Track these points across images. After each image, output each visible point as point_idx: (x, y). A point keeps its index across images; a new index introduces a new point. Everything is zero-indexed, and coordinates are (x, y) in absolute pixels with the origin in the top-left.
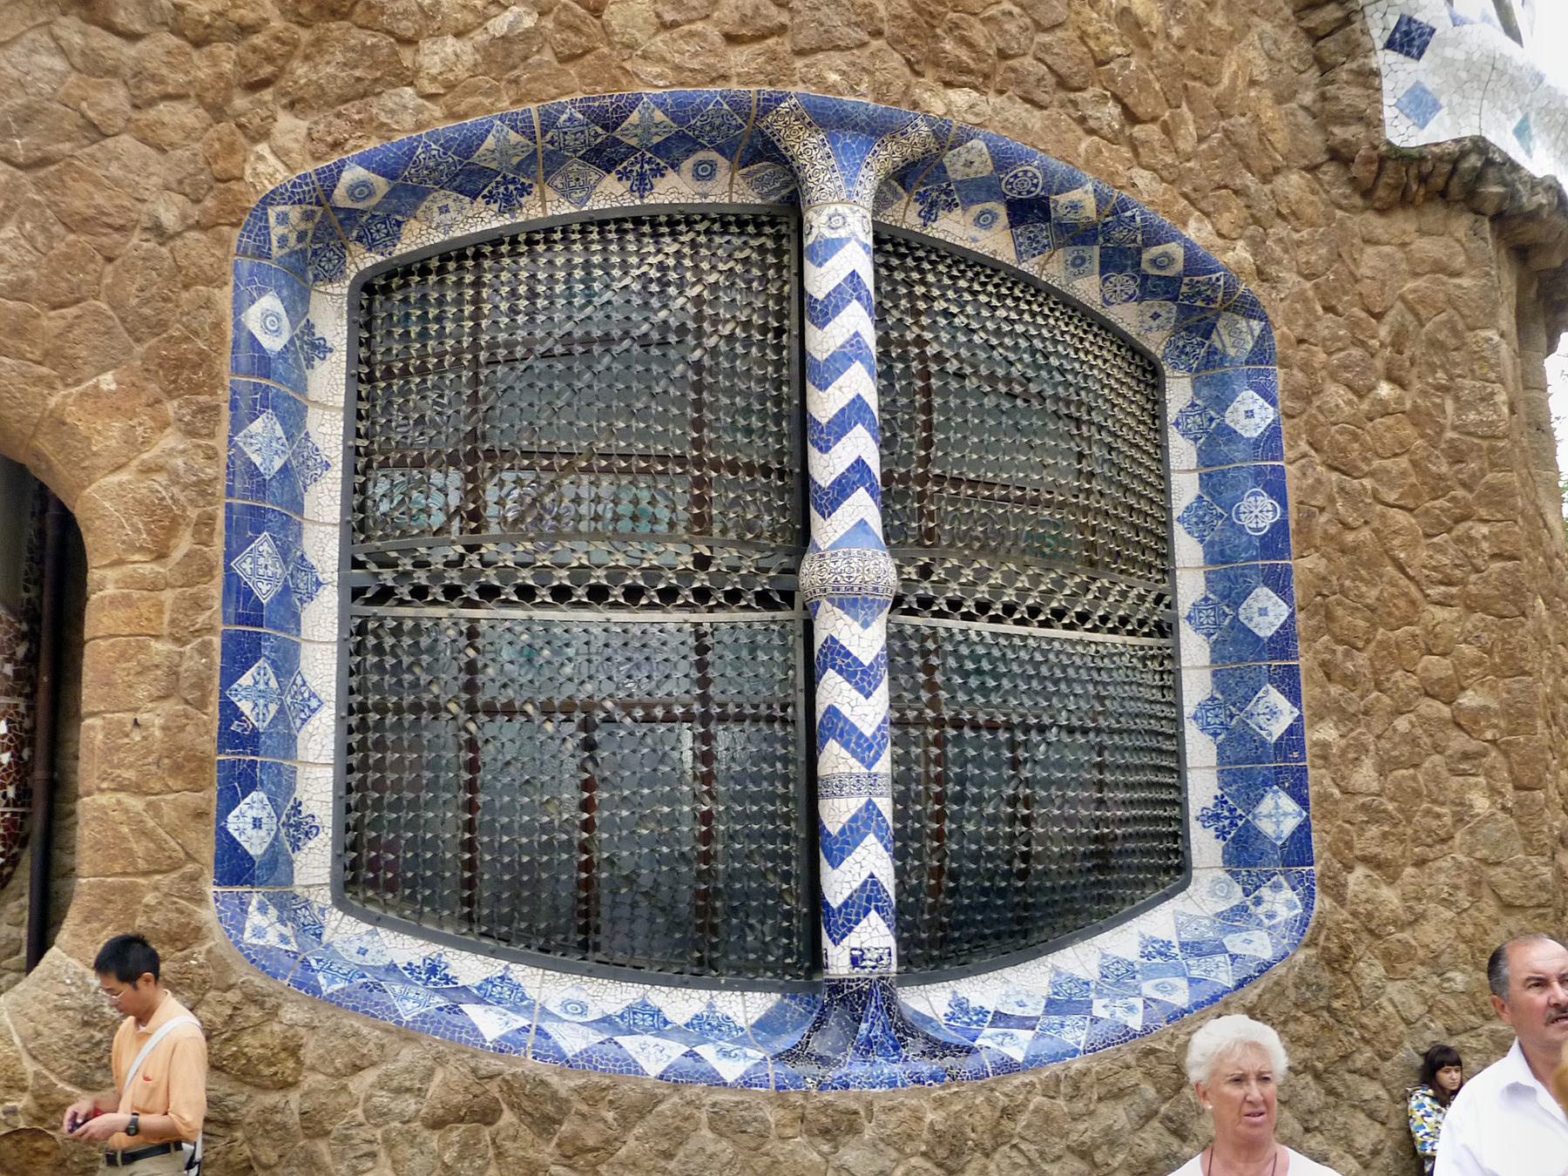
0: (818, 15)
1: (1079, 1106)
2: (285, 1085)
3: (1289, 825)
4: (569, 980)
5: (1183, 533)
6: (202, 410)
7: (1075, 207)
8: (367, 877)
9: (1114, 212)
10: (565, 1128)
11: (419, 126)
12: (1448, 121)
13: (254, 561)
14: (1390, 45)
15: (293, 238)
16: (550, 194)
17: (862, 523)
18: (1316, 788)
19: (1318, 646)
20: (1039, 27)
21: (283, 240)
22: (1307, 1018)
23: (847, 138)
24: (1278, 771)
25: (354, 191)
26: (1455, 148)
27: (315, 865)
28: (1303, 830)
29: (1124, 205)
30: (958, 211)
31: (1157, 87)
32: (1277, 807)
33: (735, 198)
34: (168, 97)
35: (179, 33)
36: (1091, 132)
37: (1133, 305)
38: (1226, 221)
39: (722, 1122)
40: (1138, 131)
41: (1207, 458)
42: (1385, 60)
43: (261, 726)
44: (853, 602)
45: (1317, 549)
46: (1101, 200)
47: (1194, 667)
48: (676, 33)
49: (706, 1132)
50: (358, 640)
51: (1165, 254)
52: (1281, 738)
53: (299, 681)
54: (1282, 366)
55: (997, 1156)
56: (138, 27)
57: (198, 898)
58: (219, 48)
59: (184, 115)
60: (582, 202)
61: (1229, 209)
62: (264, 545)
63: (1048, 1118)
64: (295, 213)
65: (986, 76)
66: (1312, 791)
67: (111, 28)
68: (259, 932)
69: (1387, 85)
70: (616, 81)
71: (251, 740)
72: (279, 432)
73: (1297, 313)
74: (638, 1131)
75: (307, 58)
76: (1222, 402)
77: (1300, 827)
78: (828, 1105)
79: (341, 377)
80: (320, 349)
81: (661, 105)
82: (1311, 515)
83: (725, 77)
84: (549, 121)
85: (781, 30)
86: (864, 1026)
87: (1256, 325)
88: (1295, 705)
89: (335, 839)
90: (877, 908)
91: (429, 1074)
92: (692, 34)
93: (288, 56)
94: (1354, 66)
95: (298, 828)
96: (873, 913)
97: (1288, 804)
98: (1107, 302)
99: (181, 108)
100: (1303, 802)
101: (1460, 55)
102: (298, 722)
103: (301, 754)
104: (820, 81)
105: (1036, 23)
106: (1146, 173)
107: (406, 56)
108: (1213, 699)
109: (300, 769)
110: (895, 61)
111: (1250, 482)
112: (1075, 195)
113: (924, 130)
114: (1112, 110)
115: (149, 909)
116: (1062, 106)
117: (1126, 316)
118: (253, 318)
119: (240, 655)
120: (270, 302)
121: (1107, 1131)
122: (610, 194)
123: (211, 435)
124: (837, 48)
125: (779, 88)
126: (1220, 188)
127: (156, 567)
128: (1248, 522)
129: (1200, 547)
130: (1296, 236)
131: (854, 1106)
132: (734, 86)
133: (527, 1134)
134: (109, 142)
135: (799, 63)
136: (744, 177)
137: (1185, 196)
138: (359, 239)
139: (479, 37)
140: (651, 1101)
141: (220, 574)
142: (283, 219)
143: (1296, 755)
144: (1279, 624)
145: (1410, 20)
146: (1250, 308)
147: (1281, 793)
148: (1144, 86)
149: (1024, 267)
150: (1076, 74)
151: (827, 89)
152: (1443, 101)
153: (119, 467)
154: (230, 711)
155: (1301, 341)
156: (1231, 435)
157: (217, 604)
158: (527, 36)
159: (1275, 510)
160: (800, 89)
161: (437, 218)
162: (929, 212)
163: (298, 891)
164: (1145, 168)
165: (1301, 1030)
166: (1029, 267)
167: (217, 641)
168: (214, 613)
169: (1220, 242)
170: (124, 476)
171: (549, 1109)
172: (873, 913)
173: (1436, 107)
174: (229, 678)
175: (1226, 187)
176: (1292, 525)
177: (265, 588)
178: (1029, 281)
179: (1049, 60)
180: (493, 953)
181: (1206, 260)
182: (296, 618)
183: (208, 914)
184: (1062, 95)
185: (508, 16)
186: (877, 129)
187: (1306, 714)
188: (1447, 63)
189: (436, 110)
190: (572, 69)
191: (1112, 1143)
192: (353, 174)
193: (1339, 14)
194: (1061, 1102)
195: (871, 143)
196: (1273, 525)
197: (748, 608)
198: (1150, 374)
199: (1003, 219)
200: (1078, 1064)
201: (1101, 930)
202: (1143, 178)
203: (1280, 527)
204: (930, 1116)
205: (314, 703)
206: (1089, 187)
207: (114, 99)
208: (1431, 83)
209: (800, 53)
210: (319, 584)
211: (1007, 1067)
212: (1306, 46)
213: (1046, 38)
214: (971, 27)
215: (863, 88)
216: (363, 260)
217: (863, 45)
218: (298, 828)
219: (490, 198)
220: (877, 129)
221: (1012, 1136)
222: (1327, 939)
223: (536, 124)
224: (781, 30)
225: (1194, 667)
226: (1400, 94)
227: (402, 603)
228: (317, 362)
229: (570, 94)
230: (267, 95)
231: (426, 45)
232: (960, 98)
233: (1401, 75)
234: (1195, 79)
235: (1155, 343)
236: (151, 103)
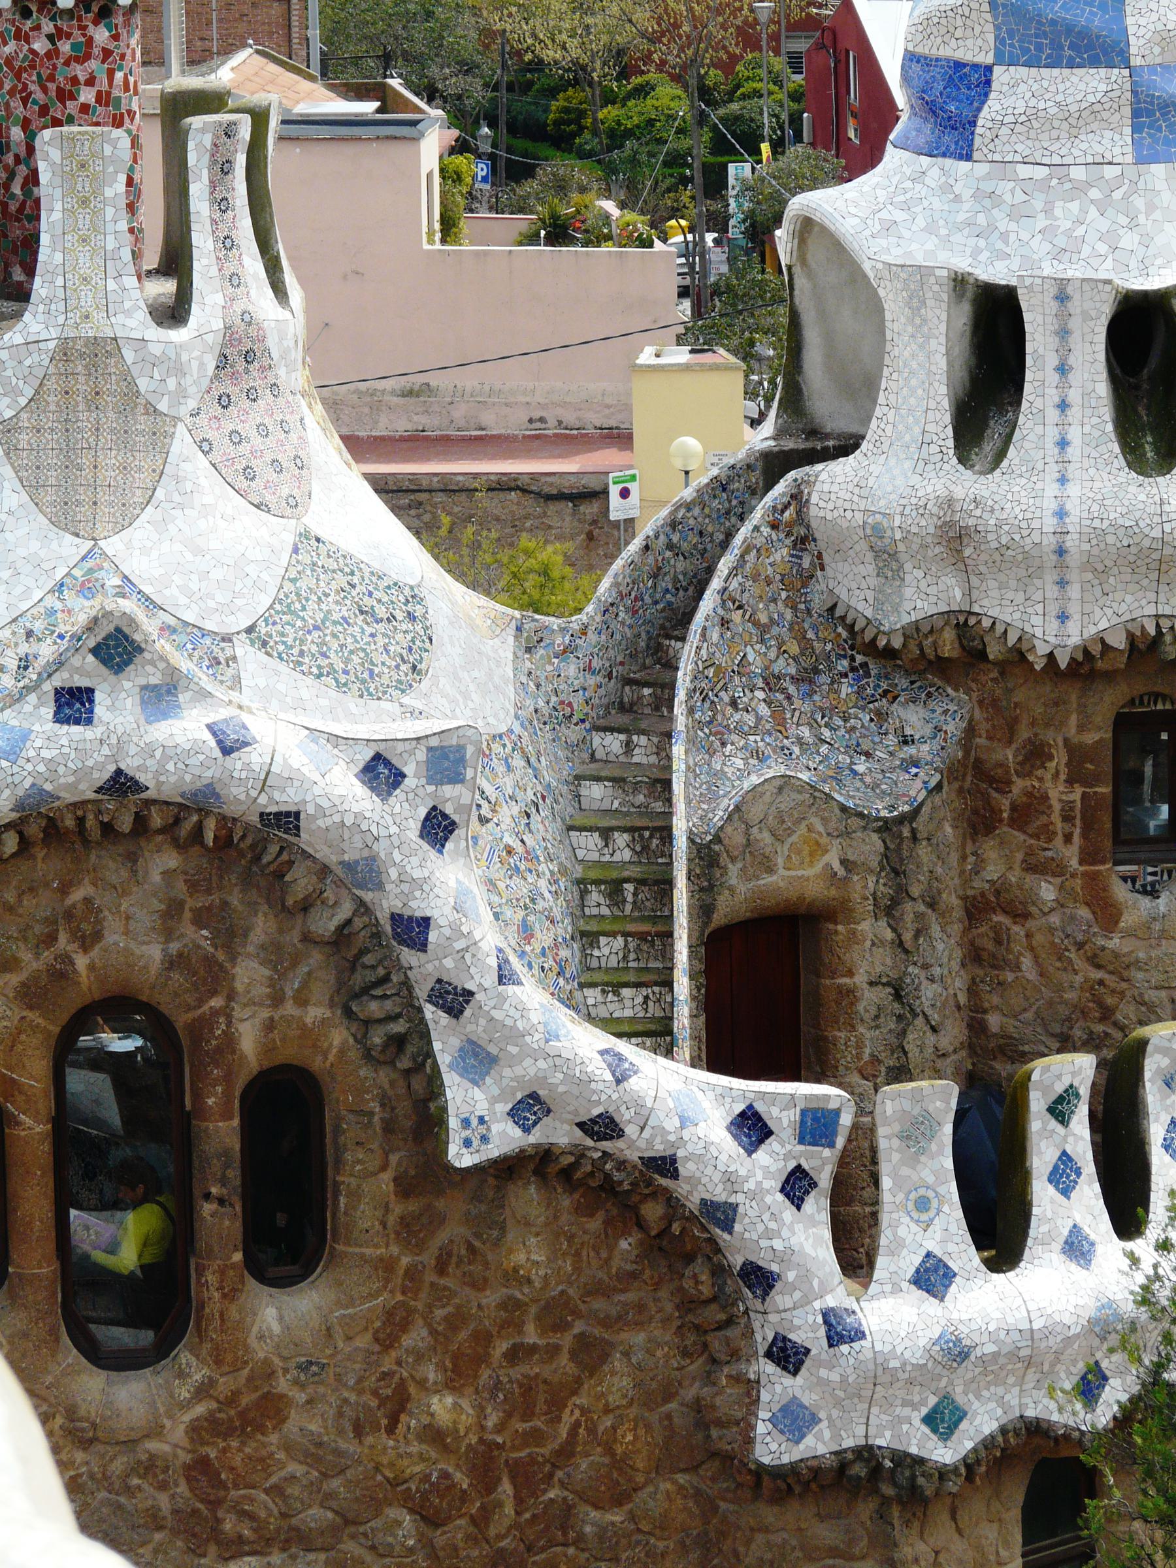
12: (827, 1434)
14: (769, 1355)
26: (830, 1462)
69: (765, 1396)
101: (835, 1377)
145: (785, 1338)
152: (822, 1415)
173: (814, 1420)
193: (722, 1316)
208: (807, 1399)
233: (778, 1388)
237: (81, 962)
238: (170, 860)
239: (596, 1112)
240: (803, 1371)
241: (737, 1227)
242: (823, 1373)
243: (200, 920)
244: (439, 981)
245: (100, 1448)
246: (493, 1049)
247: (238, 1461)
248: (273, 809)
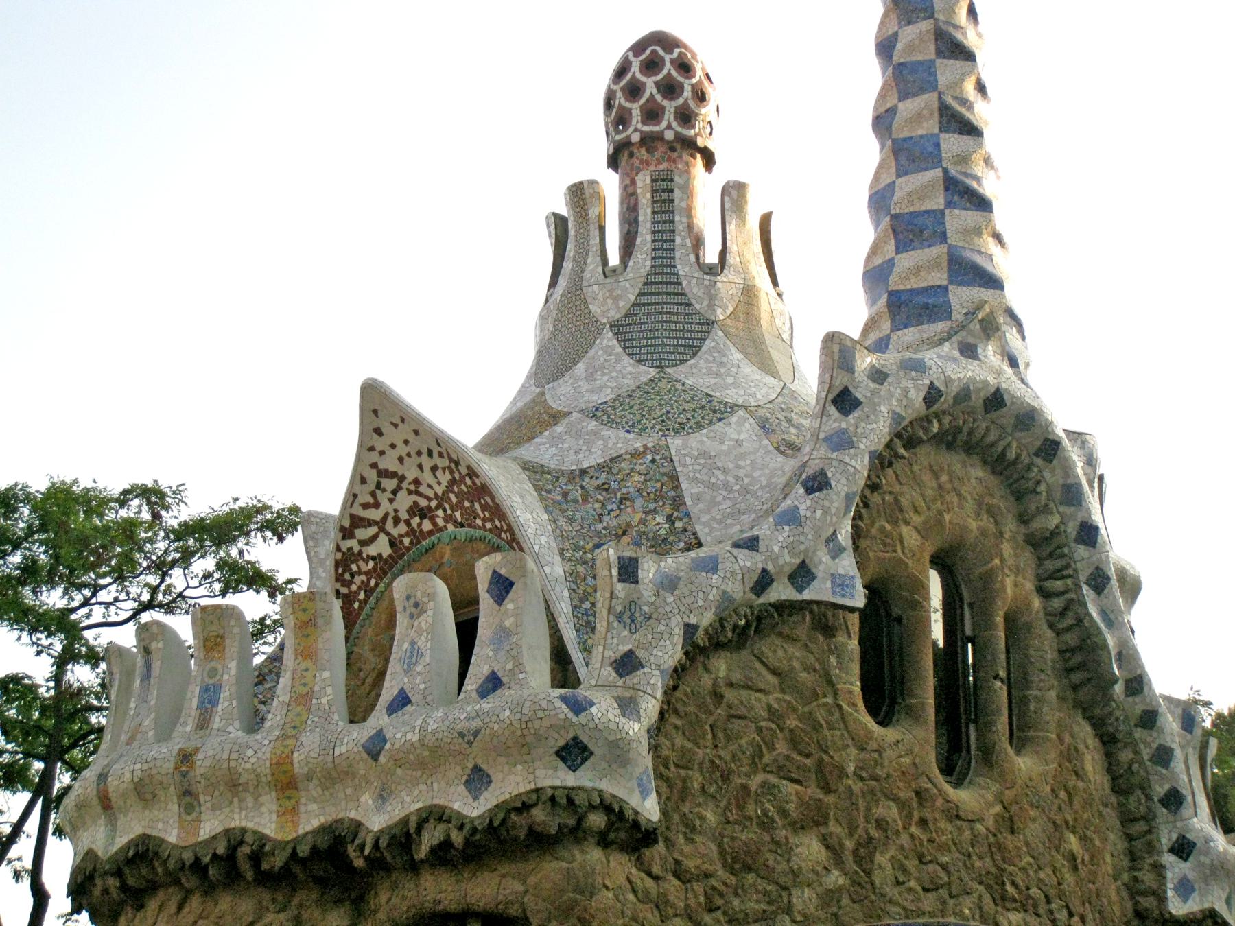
12: (1197, 899)
14: (1172, 850)
20: (1040, 868)
26: (1200, 916)
34: (676, 915)
35: (677, 875)
42: (1169, 859)
58: (696, 886)
69: (1169, 875)
75: (736, 895)
92: (910, 890)
94: (1151, 861)
107: (784, 894)
110: (987, 899)
114: (1065, 913)
152: (1196, 886)
188: (1201, 865)
193: (1146, 828)
208: (1191, 876)
212: (1126, 845)
213: (1042, 875)
226: (1176, 881)
230: (719, 914)
233: (1177, 870)
237: (947, 517)
238: (980, 474)
239: (1139, 672)
240: (1191, 858)
241: (1172, 765)
242: (1202, 858)
243: (990, 511)
244: (1097, 568)
245: (959, 823)
246: (1112, 617)
248: (1051, 437)
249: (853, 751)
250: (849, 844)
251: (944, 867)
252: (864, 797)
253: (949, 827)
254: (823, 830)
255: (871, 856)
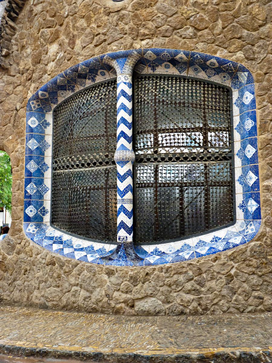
0: (112, 34)
1: (168, 275)
2: (31, 257)
3: (254, 208)
4: (81, 240)
5: (236, 132)
6: (22, 140)
7: (181, 58)
8: (53, 222)
9: (191, 57)
10: (64, 268)
11: (48, 81)
13: (30, 165)
15: (37, 106)
16: (79, 86)
17: (122, 145)
18: (264, 198)
19: (267, 159)
21: (34, 107)
22: (254, 260)
23: (121, 60)
24: (252, 194)
25: (42, 95)
27: (47, 218)
28: (259, 209)
29: (193, 54)
30: (160, 66)
31: (207, 19)
32: (251, 204)
33: (111, 77)
34: (18, 86)
35: (19, 73)
36: (184, 38)
37: (217, 76)
38: (232, 48)
39: (89, 269)
40: (199, 33)
41: (241, 111)
43: (32, 194)
44: (123, 162)
45: (268, 131)
46: (187, 55)
47: (238, 167)
48: (85, 49)
49: (85, 271)
50: (55, 177)
51: (211, 63)
52: (252, 185)
53: (44, 185)
54: (258, 82)
55: (146, 284)
56: (14, 74)
57: (22, 224)
59: (20, 88)
60: (84, 86)
61: (234, 44)
62: (32, 162)
63: (158, 277)
64: (35, 102)
65: (152, 34)
66: (262, 199)
67: (11, 75)
68: (29, 230)
70: (75, 62)
71: (30, 196)
72: (35, 141)
73: (265, 65)
74: (75, 269)
76: (242, 96)
77: (257, 209)
78: (107, 268)
79: (52, 129)
80: (48, 124)
81: (83, 65)
82: (266, 122)
83: (94, 55)
84: (66, 75)
85: (105, 40)
86: (119, 253)
87: (246, 73)
88: (256, 176)
89: (51, 214)
90: (123, 228)
91: (47, 256)
92: (87, 48)
93: (33, 73)
95: (44, 212)
96: (122, 229)
97: (254, 203)
98: (209, 77)
99: (20, 87)
100: (258, 202)
102: (44, 193)
103: (45, 198)
104: (112, 50)
105: (167, 16)
106: (203, 43)
108: (242, 175)
109: (45, 201)
111: (247, 117)
112: (179, 56)
113: (136, 53)
114: (191, 29)
115: (17, 226)
116: (176, 34)
117: (217, 79)
118: (29, 123)
119: (28, 182)
120: (33, 119)
121: (175, 282)
122: (89, 83)
123: (24, 144)
124: (116, 40)
125: (104, 54)
126: (231, 39)
127: (17, 168)
128: (246, 127)
129: (240, 135)
130: (268, 43)
131: (113, 269)
132: (96, 56)
133: (59, 268)
134: (10, 96)
135: (108, 47)
136: (111, 72)
137: (217, 45)
138: (52, 103)
139: (56, 60)
140: (77, 265)
141: (25, 168)
142: (33, 103)
143: (256, 189)
144: (252, 154)
146: (243, 69)
147: (252, 200)
148: (202, 20)
149: (182, 74)
150: (178, 25)
151: (115, 50)
153: (13, 152)
154: (26, 192)
155: (266, 74)
156: (243, 104)
157: (24, 173)
158: (62, 58)
159: (252, 123)
160: (109, 52)
161: (62, 96)
162: (153, 68)
163: (44, 223)
164: (202, 42)
165: (251, 263)
166: (184, 74)
167: (24, 180)
168: (24, 176)
169: (230, 54)
170: (13, 153)
171: (61, 264)
172: (122, 229)
174: (26, 186)
175: (234, 38)
176: (258, 126)
177: (32, 170)
178: (185, 78)
179: (170, 24)
180: (70, 235)
181: (224, 60)
182: (43, 175)
183: (23, 227)
184: (175, 31)
185: (59, 55)
186: (126, 56)
187: (260, 178)
189: (50, 77)
190: (69, 62)
191: (177, 285)
192: (40, 93)
194: (163, 273)
195: (126, 59)
196: (252, 127)
197: (110, 165)
198: (228, 92)
199: (171, 65)
200: (168, 265)
201: (202, 234)
202: (200, 46)
203: (254, 128)
204: (130, 273)
205: (47, 189)
206: (182, 53)
207: (11, 88)
209: (109, 44)
210: (48, 167)
211: (150, 264)
213: (169, 19)
214: (148, 24)
215: (121, 48)
216: (54, 106)
217: (122, 37)
218: (44, 212)
219: (69, 90)
220: (126, 56)
221: (149, 280)
222: (266, 239)
223: (64, 75)
224: (105, 40)
225: (238, 167)
227: (58, 170)
228: (47, 127)
229: (68, 66)
230: (30, 81)
231: (49, 65)
232: (144, 42)
234: (224, 11)
235: (228, 83)
236: (16, 87)
247: (144, 13)
249: (67, 7)
250: (67, 41)
251: (105, 34)
252: (72, 22)
253: (107, 17)
254: (58, 40)
255: (74, 43)
